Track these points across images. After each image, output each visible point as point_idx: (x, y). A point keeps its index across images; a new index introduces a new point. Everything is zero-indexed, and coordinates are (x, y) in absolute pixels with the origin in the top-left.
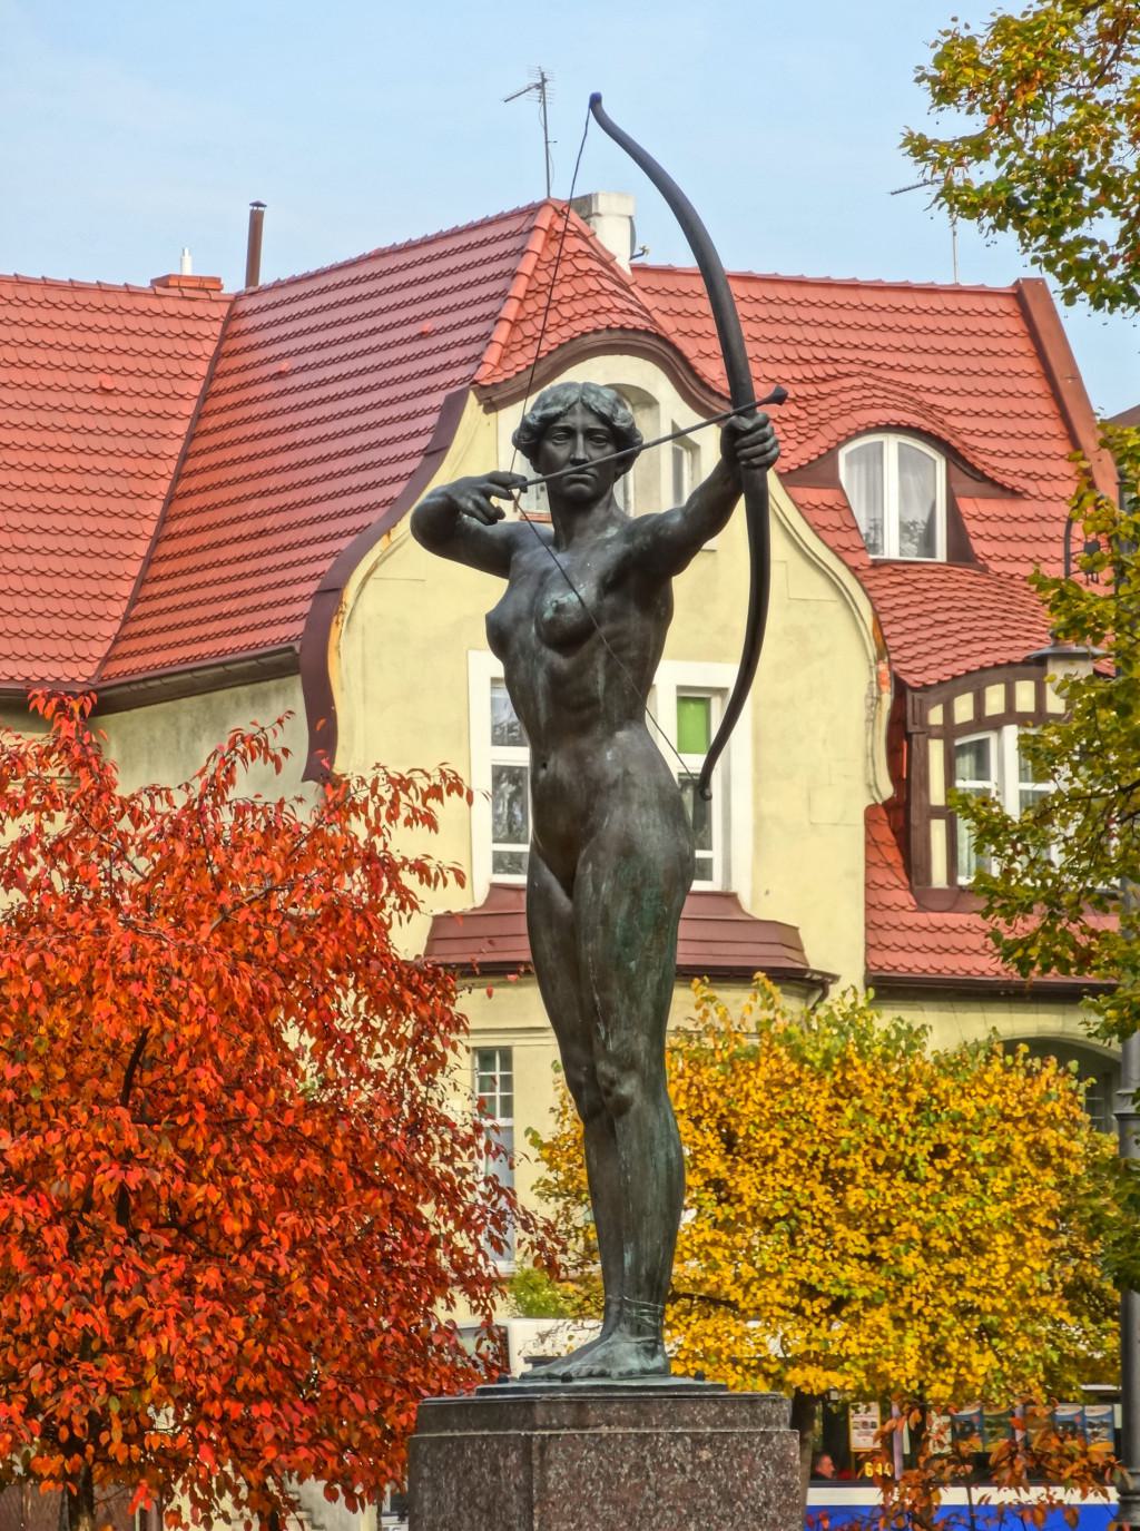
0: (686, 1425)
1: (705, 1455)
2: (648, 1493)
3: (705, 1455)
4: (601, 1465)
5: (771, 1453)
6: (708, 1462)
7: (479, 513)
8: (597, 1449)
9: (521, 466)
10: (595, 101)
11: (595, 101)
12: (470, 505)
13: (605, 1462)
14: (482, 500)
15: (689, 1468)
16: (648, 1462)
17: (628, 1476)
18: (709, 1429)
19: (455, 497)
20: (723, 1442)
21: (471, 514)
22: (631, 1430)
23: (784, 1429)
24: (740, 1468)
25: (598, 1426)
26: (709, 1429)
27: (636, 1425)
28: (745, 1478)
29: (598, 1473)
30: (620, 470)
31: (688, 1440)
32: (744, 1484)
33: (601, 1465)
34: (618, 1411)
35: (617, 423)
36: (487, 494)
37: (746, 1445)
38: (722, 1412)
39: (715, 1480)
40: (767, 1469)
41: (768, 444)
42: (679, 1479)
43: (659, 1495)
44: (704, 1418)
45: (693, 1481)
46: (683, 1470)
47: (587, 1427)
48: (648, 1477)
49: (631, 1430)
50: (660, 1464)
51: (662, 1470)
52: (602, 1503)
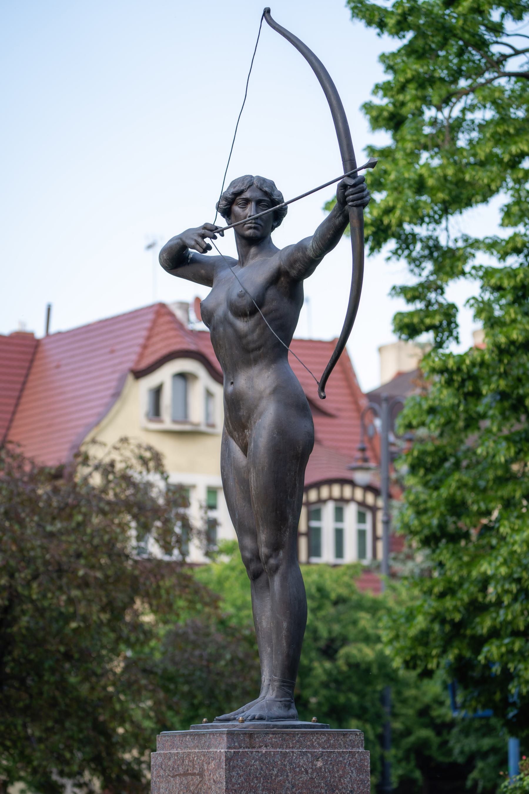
0: (308, 747)
1: (319, 764)
2: (288, 785)
3: (319, 764)
4: (262, 769)
5: (355, 763)
6: (321, 768)
7: (198, 247)
8: (260, 760)
9: (222, 222)
10: (267, 12)
11: (267, 12)
12: (193, 243)
13: (264, 768)
14: (199, 240)
15: (310, 771)
16: (288, 767)
17: (277, 776)
18: (321, 750)
19: (184, 239)
20: (329, 757)
21: (193, 248)
22: (278, 750)
23: (361, 750)
24: (338, 771)
25: (260, 747)
26: (321, 750)
27: (281, 746)
28: (340, 777)
29: (260, 774)
30: (275, 224)
31: (309, 755)
32: (340, 780)
33: (262, 769)
34: (271, 738)
35: (275, 197)
36: (203, 237)
37: (341, 759)
38: (329, 740)
39: (324, 778)
40: (352, 772)
41: (365, 193)
42: (305, 777)
43: (293, 787)
44: (318, 743)
45: (312, 778)
46: (307, 772)
47: (254, 747)
48: (287, 776)
49: (278, 750)
50: (294, 769)
51: (295, 771)
52: (263, 790)
